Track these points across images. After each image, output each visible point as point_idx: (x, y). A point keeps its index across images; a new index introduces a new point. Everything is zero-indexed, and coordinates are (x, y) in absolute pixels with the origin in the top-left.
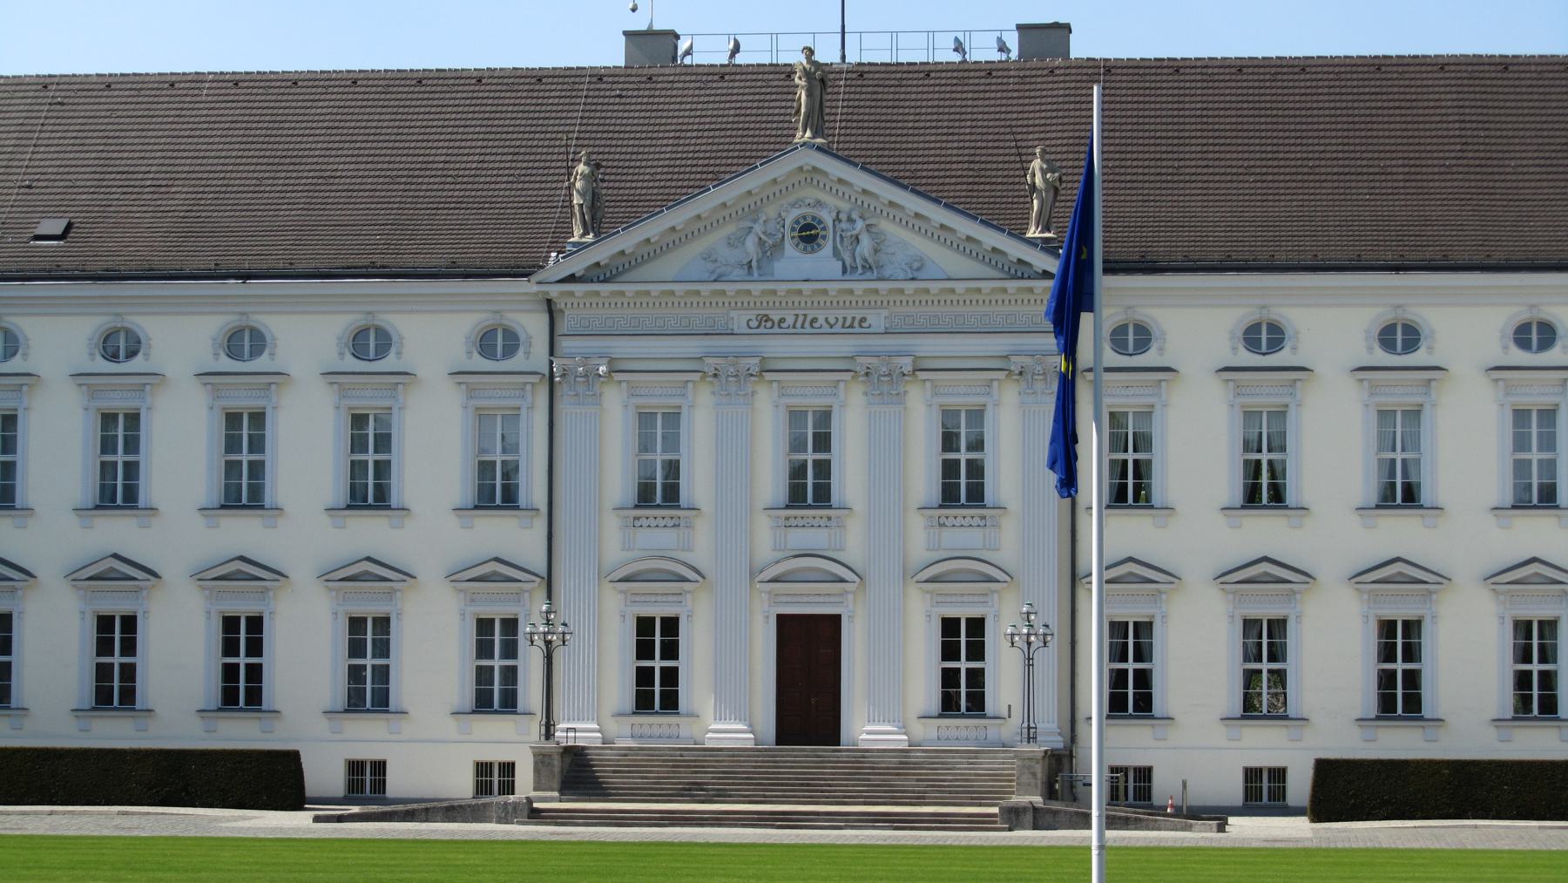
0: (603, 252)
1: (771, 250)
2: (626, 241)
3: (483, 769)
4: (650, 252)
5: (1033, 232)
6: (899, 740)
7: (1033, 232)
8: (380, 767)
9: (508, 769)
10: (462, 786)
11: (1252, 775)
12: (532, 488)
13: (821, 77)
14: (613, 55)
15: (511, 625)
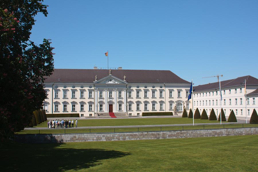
0: (98, 81)
1: (108, 82)
2: (99, 81)
3: (90, 114)
4: (101, 81)
5: (124, 81)
6: (117, 112)
7: (124, 81)
8: (83, 114)
9: (92, 114)
10: (89, 116)
11: (138, 114)
12: (93, 97)
13: (112, 70)
14: (94, 68)
15: (91, 105)
